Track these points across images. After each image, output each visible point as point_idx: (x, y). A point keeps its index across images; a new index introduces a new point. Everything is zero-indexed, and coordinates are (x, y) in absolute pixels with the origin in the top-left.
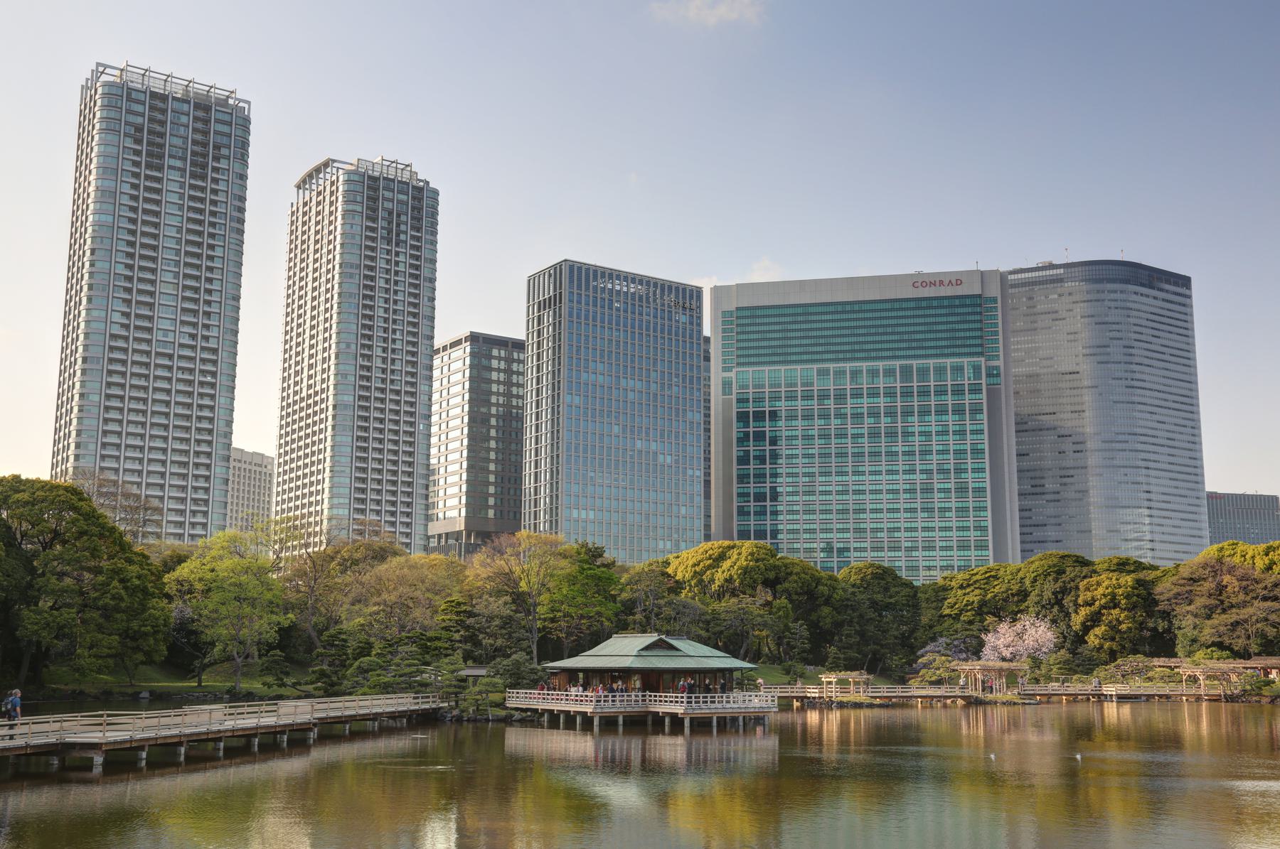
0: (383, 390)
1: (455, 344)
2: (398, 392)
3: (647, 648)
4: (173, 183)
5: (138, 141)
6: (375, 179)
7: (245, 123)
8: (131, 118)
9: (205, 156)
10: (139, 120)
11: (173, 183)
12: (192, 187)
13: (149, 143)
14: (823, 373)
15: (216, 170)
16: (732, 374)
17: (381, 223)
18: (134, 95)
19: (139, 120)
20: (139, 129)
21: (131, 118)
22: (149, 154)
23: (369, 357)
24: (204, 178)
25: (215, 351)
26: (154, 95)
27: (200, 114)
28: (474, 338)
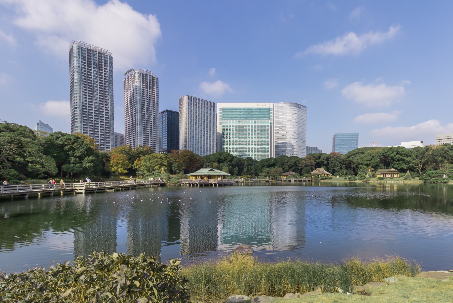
1: (164, 112)
4: (95, 72)
5: (85, 60)
6: (144, 74)
7: (111, 58)
8: (82, 55)
9: (102, 65)
10: (84, 55)
11: (95, 72)
12: (99, 72)
15: (105, 69)
16: (222, 121)
18: (83, 49)
20: (85, 57)
21: (82, 55)
22: (88, 64)
24: (102, 70)
25: (108, 110)
26: (88, 49)
28: (167, 111)
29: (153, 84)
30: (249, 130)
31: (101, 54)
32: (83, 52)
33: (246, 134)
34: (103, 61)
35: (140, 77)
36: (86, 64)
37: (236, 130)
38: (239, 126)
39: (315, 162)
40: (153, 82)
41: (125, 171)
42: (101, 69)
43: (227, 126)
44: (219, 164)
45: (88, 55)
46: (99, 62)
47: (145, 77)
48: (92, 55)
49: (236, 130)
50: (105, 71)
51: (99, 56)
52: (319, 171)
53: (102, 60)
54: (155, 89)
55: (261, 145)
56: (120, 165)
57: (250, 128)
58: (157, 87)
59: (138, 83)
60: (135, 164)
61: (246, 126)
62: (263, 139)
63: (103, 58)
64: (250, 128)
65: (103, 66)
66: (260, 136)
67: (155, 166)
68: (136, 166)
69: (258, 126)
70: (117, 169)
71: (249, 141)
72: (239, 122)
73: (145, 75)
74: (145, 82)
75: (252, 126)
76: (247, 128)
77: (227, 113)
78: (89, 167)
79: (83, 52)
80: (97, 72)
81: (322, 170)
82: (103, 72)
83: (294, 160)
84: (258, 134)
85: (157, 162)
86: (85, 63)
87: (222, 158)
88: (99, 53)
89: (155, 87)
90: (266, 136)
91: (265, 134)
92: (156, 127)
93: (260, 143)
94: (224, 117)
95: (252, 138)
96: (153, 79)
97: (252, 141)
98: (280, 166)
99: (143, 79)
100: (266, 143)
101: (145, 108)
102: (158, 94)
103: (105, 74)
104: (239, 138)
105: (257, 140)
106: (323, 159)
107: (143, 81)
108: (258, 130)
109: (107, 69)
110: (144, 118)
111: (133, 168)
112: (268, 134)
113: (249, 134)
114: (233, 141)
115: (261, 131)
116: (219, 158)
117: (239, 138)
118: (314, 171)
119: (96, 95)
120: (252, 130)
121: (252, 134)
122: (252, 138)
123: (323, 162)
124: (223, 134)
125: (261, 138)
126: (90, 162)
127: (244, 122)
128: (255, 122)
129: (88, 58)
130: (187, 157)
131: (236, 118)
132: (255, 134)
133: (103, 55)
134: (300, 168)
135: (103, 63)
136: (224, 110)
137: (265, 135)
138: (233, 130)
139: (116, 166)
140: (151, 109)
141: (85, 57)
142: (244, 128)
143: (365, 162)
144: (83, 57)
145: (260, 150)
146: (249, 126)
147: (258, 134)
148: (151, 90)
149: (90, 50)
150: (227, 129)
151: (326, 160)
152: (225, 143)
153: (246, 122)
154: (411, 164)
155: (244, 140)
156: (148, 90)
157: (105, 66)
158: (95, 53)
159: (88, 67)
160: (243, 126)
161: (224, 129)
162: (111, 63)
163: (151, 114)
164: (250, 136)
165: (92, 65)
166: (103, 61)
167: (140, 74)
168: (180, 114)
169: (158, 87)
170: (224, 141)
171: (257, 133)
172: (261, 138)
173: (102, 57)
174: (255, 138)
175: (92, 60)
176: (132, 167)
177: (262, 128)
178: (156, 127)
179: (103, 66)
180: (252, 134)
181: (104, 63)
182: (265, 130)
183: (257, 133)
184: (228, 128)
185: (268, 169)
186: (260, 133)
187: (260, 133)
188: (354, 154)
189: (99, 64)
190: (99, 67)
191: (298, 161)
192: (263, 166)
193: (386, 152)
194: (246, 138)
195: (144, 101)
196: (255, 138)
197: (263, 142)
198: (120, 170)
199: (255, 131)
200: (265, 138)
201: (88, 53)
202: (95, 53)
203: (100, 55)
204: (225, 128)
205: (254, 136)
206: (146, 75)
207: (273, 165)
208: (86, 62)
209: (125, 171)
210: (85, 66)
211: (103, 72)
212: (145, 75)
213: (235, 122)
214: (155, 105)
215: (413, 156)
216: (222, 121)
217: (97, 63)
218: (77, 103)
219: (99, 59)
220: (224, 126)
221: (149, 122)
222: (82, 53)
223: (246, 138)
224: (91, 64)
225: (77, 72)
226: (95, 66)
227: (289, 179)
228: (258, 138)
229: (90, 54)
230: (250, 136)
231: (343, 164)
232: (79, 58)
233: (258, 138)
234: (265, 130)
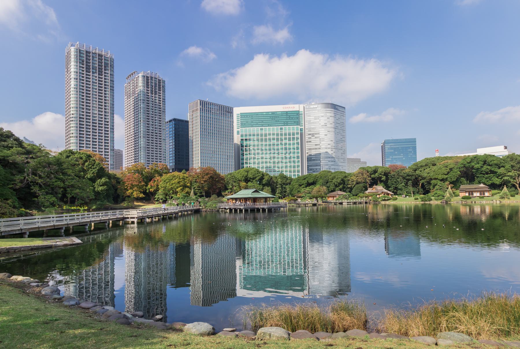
0: (153, 133)
1: (170, 121)
2: (157, 133)
3: (253, 192)
4: (94, 77)
5: (83, 65)
7: (112, 60)
8: (81, 58)
9: (102, 69)
10: (83, 58)
13: (86, 65)
15: (105, 73)
16: (239, 130)
17: (149, 89)
18: (81, 52)
19: (83, 58)
21: (81, 58)
22: (86, 68)
23: (148, 124)
24: (102, 75)
25: (108, 122)
26: (87, 52)
27: (100, 58)
28: (175, 120)
29: (160, 88)
30: (274, 139)
31: (102, 56)
32: (82, 55)
33: (270, 145)
34: (103, 64)
35: (144, 81)
36: (85, 69)
37: (258, 140)
38: (262, 135)
39: (370, 178)
40: (159, 85)
41: (142, 195)
42: (100, 74)
43: (246, 135)
44: (247, 183)
45: (86, 59)
46: (99, 65)
47: (150, 81)
48: (91, 58)
49: (258, 140)
50: (105, 76)
51: (99, 59)
52: (377, 189)
53: (102, 63)
54: (161, 94)
55: (290, 158)
56: (136, 188)
57: (275, 137)
58: (164, 92)
59: (141, 88)
60: (149, 186)
61: (270, 135)
62: (292, 151)
63: (103, 61)
64: (275, 137)
65: (103, 70)
67: (177, 188)
68: (151, 188)
69: (285, 134)
70: (132, 193)
71: (274, 153)
73: (150, 78)
74: (150, 86)
75: (277, 135)
76: (272, 137)
77: (248, 120)
78: (102, 191)
79: (82, 55)
80: (96, 77)
81: (380, 188)
82: (103, 77)
83: (341, 177)
85: (179, 183)
86: (83, 68)
87: (250, 176)
88: (99, 55)
89: (161, 92)
90: (296, 146)
91: (294, 144)
92: (162, 140)
93: (288, 156)
94: (243, 125)
95: (278, 149)
96: (159, 83)
97: (278, 154)
98: (323, 185)
99: (148, 83)
100: (296, 155)
101: (150, 118)
102: (164, 99)
103: (105, 79)
104: (262, 150)
105: (284, 152)
106: (380, 174)
107: (148, 85)
108: (286, 139)
109: (108, 73)
110: (149, 130)
111: (147, 191)
112: (298, 143)
113: (274, 145)
114: (254, 154)
116: (247, 176)
117: (262, 150)
118: (370, 190)
119: (94, 104)
120: (278, 139)
121: (277, 145)
122: (278, 149)
123: (381, 177)
124: (242, 146)
125: (290, 149)
126: (103, 185)
127: (268, 130)
128: (281, 129)
129: (86, 62)
130: (209, 176)
131: (257, 125)
132: (281, 144)
133: (103, 58)
134: (349, 186)
135: (103, 67)
136: (243, 116)
137: (294, 144)
138: (254, 140)
139: (131, 188)
140: (156, 119)
141: (83, 61)
142: (268, 137)
143: (440, 177)
144: (81, 61)
145: (288, 164)
147: (286, 144)
148: (157, 96)
149: (89, 53)
150: (246, 140)
151: (384, 175)
152: (245, 157)
153: (269, 130)
154: (506, 178)
155: (268, 152)
156: (154, 95)
157: (105, 70)
158: (94, 55)
159: (86, 72)
160: (266, 135)
161: (242, 140)
162: (112, 66)
163: (156, 124)
164: (276, 147)
165: (91, 70)
166: (103, 64)
167: (144, 76)
168: (190, 123)
169: (165, 92)
170: (243, 155)
171: (283, 143)
172: (290, 149)
173: (102, 60)
174: (282, 149)
175: (91, 64)
176: (146, 190)
177: (291, 137)
178: (162, 140)
179: (103, 70)
180: (277, 145)
181: (105, 67)
182: (293, 138)
183: (283, 143)
184: (248, 138)
185: (308, 189)
186: (288, 142)
187: (288, 142)
188: (422, 166)
189: (99, 68)
190: (99, 71)
191: (346, 177)
192: (300, 185)
193: (468, 163)
194: (270, 150)
195: (149, 109)
196: (282, 149)
197: (292, 155)
198: (135, 194)
199: (282, 140)
200: (294, 149)
201: (86, 55)
202: (94, 55)
203: (100, 58)
204: (244, 138)
205: (280, 147)
206: (152, 78)
207: (314, 183)
208: (85, 66)
209: (142, 195)
210: (83, 71)
211: (103, 77)
212: (150, 78)
213: (255, 130)
214: (162, 111)
215: (508, 166)
216: (239, 130)
217: (96, 67)
218: (73, 114)
219: (99, 62)
220: (242, 136)
221: (154, 134)
222: (80, 56)
224: (90, 69)
225: (74, 79)
226: (95, 71)
227: (340, 201)
228: (286, 149)
229: (90, 56)
230: (276, 147)
231: (408, 180)
232: (77, 62)
233: (286, 149)
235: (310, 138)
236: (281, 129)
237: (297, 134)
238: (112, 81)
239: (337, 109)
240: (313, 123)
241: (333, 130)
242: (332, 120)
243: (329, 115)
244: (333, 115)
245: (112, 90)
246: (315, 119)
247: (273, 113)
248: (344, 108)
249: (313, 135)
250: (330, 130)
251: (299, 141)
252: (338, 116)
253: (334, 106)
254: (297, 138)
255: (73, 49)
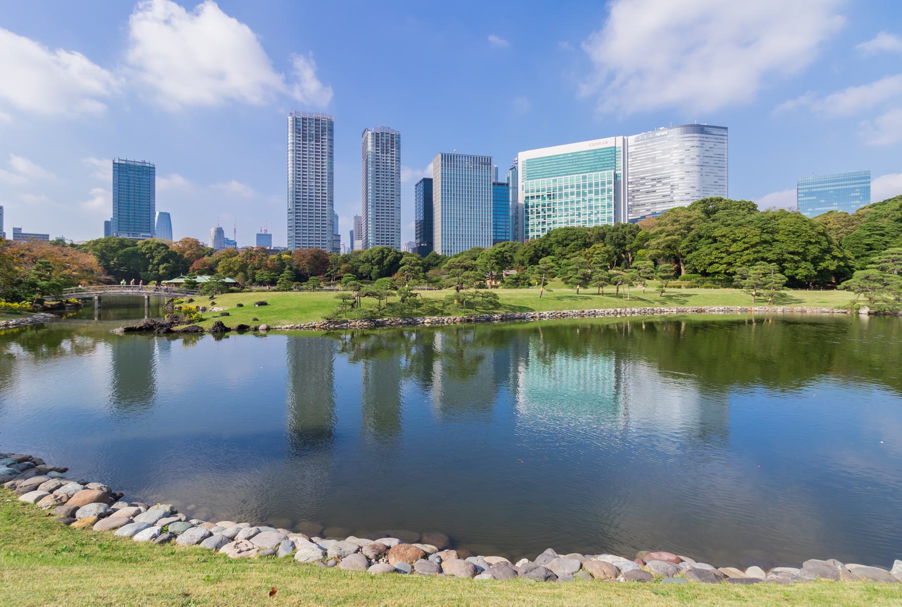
4: (311, 145)
7: (331, 124)
14: (555, 181)
30: (572, 194)
33: (566, 203)
35: (373, 139)
57: (575, 190)
58: (399, 148)
61: (566, 187)
62: (600, 209)
64: (575, 190)
66: (593, 202)
71: (573, 215)
72: (555, 181)
75: (578, 187)
76: (569, 190)
77: (537, 169)
84: (590, 200)
90: (606, 201)
94: (530, 176)
95: (578, 209)
97: (579, 215)
107: (377, 143)
108: (590, 192)
112: (609, 198)
115: (597, 193)
120: (578, 194)
121: (578, 202)
124: (527, 207)
131: (550, 175)
132: (584, 200)
142: (564, 191)
146: (572, 187)
147: (590, 200)
148: (389, 155)
150: (532, 197)
152: (530, 222)
155: (564, 214)
160: (561, 189)
167: (373, 134)
170: (528, 219)
174: (585, 208)
177: (598, 188)
180: (578, 202)
182: (603, 191)
196: (585, 208)
199: (584, 194)
204: (530, 195)
205: (581, 205)
223: (566, 210)
228: (591, 207)
230: (575, 206)
233: (591, 207)
234: (603, 191)
235: (654, 186)
236: (584, 178)
237: (609, 183)
238: (331, 147)
239: (707, 133)
240: (660, 160)
241: (697, 169)
242: (694, 152)
243: (688, 144)
244: (696, 143)
245: (331, 156)
246: (664, 154)
247: (574, 154)
248: (726, 128)
249: (659, 180)
250: (691, 169)
251: (612, 193)
252: (707, 145)
253: (701, 129)
254: (609, 190)
255: (290, 118)
